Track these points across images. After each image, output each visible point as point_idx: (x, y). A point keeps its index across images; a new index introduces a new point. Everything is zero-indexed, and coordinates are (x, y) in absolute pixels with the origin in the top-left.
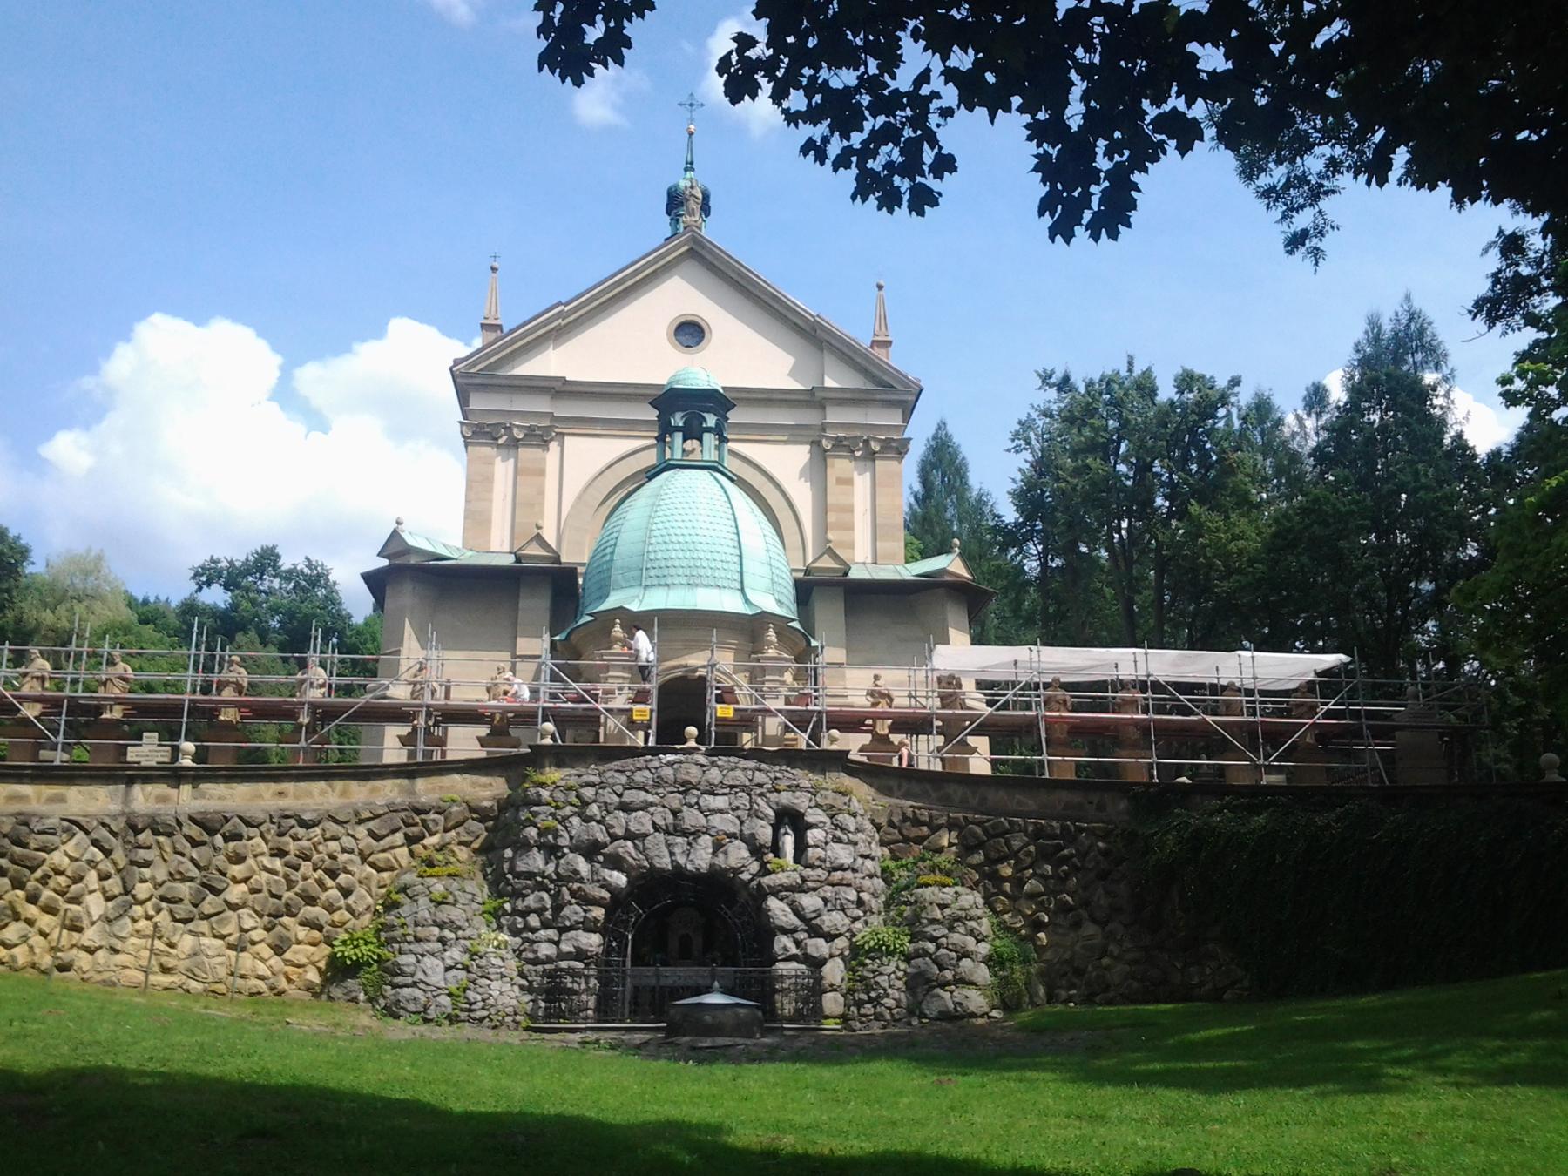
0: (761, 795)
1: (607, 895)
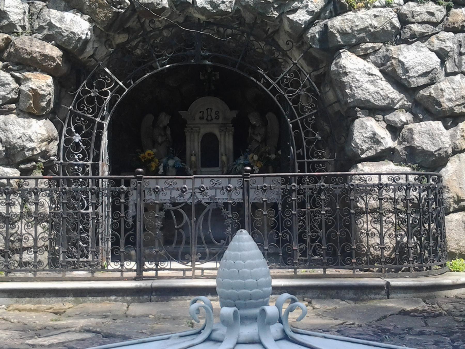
1: (54, 52)
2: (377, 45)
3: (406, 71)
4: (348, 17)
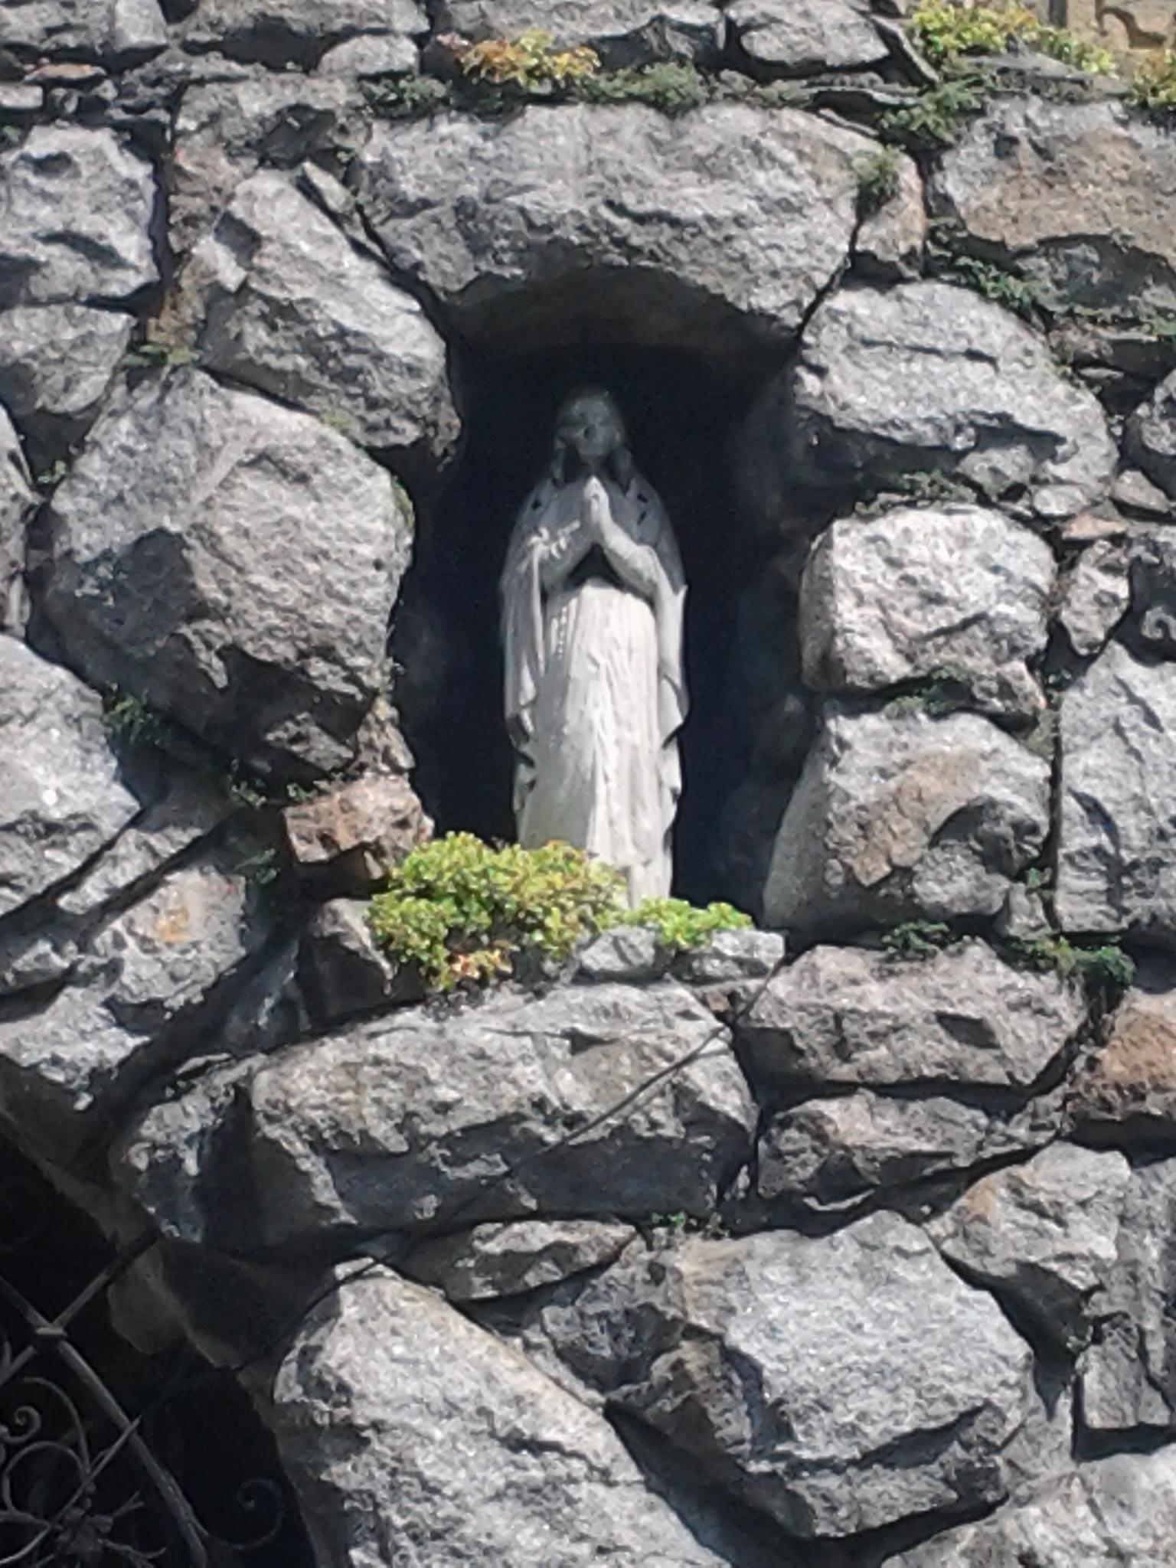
0: (294, 143)
2: (589, 1237)
3: (775, 1423)
4: (382, 1047)
